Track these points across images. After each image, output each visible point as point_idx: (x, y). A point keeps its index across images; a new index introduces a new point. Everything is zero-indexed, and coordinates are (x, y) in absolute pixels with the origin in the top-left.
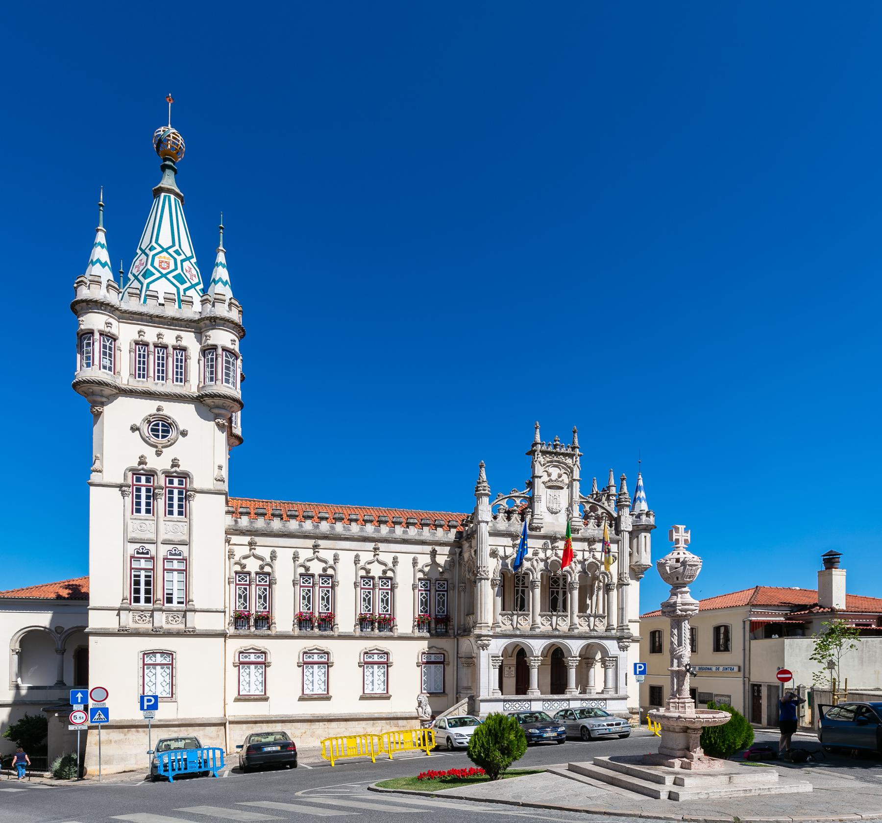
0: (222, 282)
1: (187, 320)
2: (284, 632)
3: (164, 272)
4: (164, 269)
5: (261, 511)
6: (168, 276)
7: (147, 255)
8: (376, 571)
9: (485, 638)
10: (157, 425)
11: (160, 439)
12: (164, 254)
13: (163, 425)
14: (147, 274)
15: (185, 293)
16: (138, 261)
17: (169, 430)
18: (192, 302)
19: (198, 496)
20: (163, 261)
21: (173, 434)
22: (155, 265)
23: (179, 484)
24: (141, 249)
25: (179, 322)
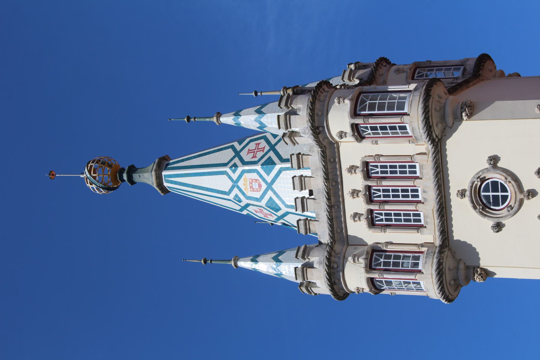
0: (261, 108)
1: (324, 161)
3: (264, 186)
4: (260, 186)
6: (269, 181)
7: (248, 205)
10: (487, 197)
11: (509, 194)
12: (241, 184)
13: (486, 189)
14: (273, 207)
16: (258, 214)
17: (492, 182)
18: (300, 153)
20: (251, 187)
22: (258, 197)
24: (241, 210)
25: (329, 171)
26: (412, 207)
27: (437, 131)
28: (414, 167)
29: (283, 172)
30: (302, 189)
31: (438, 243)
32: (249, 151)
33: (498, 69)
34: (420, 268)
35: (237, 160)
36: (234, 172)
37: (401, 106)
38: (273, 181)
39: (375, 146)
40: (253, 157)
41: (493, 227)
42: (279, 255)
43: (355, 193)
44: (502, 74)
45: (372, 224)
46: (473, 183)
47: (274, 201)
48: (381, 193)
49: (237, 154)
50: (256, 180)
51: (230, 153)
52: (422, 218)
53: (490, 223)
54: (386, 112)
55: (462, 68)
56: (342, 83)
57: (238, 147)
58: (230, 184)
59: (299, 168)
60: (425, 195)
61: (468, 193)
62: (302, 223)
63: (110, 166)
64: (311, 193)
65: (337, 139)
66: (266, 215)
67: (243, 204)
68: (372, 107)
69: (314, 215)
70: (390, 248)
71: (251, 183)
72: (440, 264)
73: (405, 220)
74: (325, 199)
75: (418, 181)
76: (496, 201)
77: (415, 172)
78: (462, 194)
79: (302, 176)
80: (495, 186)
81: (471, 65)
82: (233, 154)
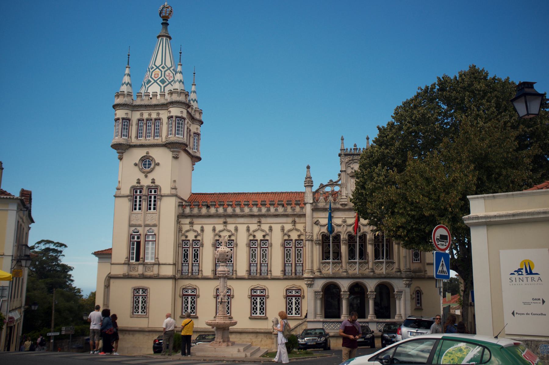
2: (247, 266)
3: (156, 79)
4: (156, 78)
5: (222, 203)
6: (157, 81)
7: (150, 72)
8: (259, 236)
9: (309, 280)
10: (146, 161)
11: (147, 169)
12: (157, 70)
13: (149, 161)
14: (149, 82)
15: (164, 90)
18: (165, 95)
19: (164, 199)
21: (152, 166)
23: (154, 193)
26: (144, 135)
27: (169, 146)
28: (158, 137)
29: (160, 87)
30: (152, 95)
31: (131, 144)
32: (169, 74)
33: (196, 163)
34: (123, 137)
35: (166, 68)
36: (162, 67)
37: (178, 134)
38: (157, 83)
39: (166, 123)
40: (167, 76)
41: (136, 163)
42: (129, 84)
43: (150, 115)
44: (194, 165)
45: (139, 120)
46: (151, 157)
47: (150, 83)
48: (149, 124)
49: (169, 69)
50: (158, 76)
51: (169, 66)
52: (140, 138)
53: (137, 163)
54: (176, 128)
55: (197, 151)
56: (194, 108)
57: (171, 69)
58: (158, 66)
59: (160, 95)
60: (148, 140)
61: (148, 155)
62: (141, 94)
63: (170, 14)
64: (151, 98)
65: (169, 110)
66: (146, 78)
67: (150, 69)
68: (179, 123)
69: (144, 98)
70: (130, 126)
71: (157, 74)
72: (124, 144)
73: (140, 132)
74: (148, 104)
75: (153, 138)
76: (145, 164)
77: (156, 137)
78: (147, 153)
79: (157, 95)
80: (150, 164)
81: (197, 155)
82: (169, 67)
